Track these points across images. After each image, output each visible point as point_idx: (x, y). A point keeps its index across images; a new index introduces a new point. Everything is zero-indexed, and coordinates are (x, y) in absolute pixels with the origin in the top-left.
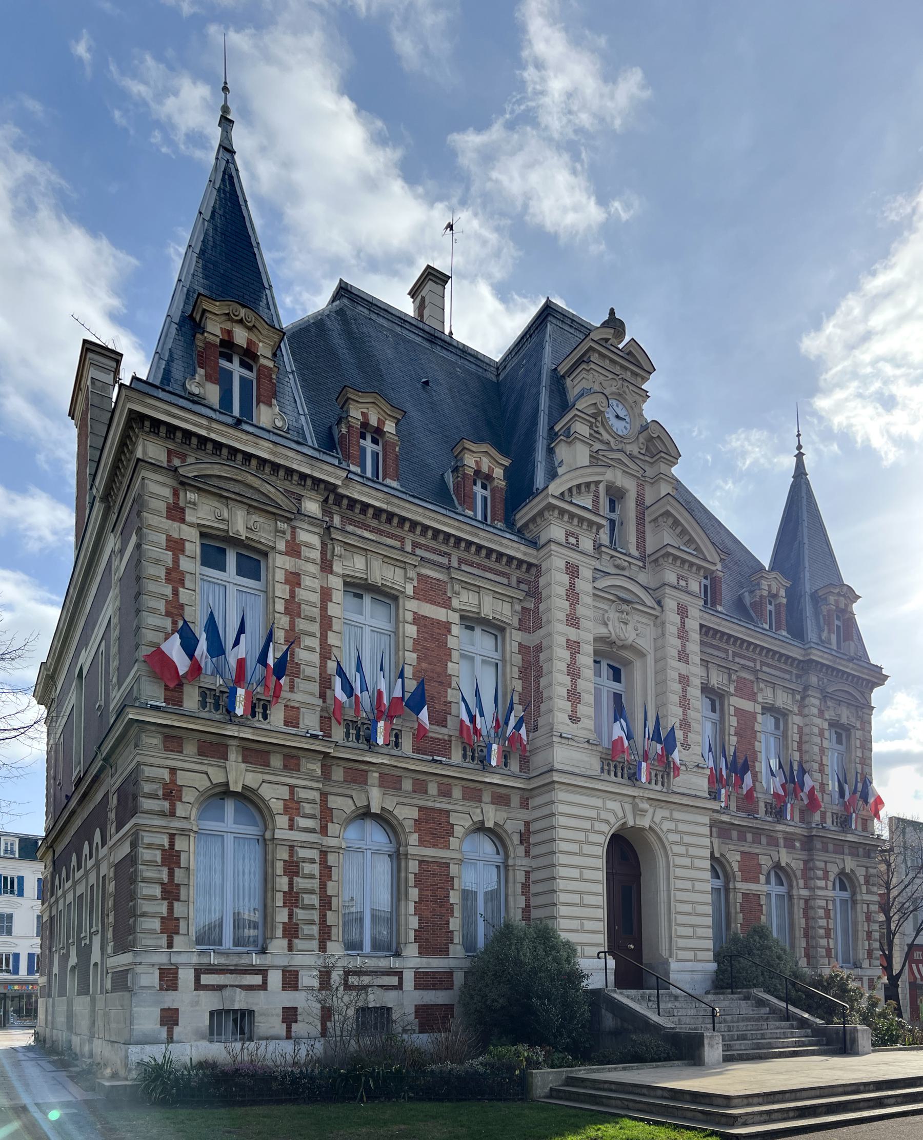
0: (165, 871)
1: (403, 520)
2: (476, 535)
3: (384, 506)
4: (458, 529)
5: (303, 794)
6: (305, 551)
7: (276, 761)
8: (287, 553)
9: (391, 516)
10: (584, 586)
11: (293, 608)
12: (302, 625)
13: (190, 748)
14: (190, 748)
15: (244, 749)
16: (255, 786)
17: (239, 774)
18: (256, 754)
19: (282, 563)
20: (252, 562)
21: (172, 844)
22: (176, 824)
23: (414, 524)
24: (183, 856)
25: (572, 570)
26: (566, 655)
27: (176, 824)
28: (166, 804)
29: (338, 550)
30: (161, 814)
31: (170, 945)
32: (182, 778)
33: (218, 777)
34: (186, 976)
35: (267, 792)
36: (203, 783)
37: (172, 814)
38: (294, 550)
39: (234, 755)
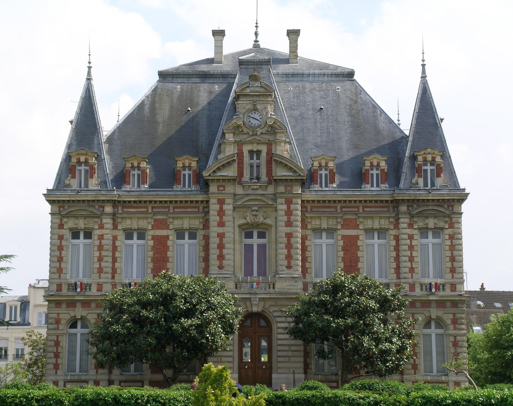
0: (55, 348)
1: (145, 202)
2: (177, 198)
3: (136, 199)
4: (169, 198)
6: (106, 226)
7: (93, 305)
8: (99, 228)
9: (140, 202)
10: (228, 207)
11: (100, 248)
12: (104, 253)
13: (64, 306)
14: (64, 306)
15: (82, 303)
16: (85, 315)
18: (86, 304)
19: (97, 233)
20: (88, 235)
21: (57, 339)
22: (58, 332)
23: (150, 202)
24: (61, 343)
25: (221, 202)
26: (217, 240)
27: (58, 332)
28: (56, 326)
29: (119, 220)
30: (54, 329)
31: (56, 373)
32: (61, 316)
33: (72, 314)
35: (89, 317)
36: (68, 317)
37: (58, 329)
38: (101, 227)
39: (79, 305)
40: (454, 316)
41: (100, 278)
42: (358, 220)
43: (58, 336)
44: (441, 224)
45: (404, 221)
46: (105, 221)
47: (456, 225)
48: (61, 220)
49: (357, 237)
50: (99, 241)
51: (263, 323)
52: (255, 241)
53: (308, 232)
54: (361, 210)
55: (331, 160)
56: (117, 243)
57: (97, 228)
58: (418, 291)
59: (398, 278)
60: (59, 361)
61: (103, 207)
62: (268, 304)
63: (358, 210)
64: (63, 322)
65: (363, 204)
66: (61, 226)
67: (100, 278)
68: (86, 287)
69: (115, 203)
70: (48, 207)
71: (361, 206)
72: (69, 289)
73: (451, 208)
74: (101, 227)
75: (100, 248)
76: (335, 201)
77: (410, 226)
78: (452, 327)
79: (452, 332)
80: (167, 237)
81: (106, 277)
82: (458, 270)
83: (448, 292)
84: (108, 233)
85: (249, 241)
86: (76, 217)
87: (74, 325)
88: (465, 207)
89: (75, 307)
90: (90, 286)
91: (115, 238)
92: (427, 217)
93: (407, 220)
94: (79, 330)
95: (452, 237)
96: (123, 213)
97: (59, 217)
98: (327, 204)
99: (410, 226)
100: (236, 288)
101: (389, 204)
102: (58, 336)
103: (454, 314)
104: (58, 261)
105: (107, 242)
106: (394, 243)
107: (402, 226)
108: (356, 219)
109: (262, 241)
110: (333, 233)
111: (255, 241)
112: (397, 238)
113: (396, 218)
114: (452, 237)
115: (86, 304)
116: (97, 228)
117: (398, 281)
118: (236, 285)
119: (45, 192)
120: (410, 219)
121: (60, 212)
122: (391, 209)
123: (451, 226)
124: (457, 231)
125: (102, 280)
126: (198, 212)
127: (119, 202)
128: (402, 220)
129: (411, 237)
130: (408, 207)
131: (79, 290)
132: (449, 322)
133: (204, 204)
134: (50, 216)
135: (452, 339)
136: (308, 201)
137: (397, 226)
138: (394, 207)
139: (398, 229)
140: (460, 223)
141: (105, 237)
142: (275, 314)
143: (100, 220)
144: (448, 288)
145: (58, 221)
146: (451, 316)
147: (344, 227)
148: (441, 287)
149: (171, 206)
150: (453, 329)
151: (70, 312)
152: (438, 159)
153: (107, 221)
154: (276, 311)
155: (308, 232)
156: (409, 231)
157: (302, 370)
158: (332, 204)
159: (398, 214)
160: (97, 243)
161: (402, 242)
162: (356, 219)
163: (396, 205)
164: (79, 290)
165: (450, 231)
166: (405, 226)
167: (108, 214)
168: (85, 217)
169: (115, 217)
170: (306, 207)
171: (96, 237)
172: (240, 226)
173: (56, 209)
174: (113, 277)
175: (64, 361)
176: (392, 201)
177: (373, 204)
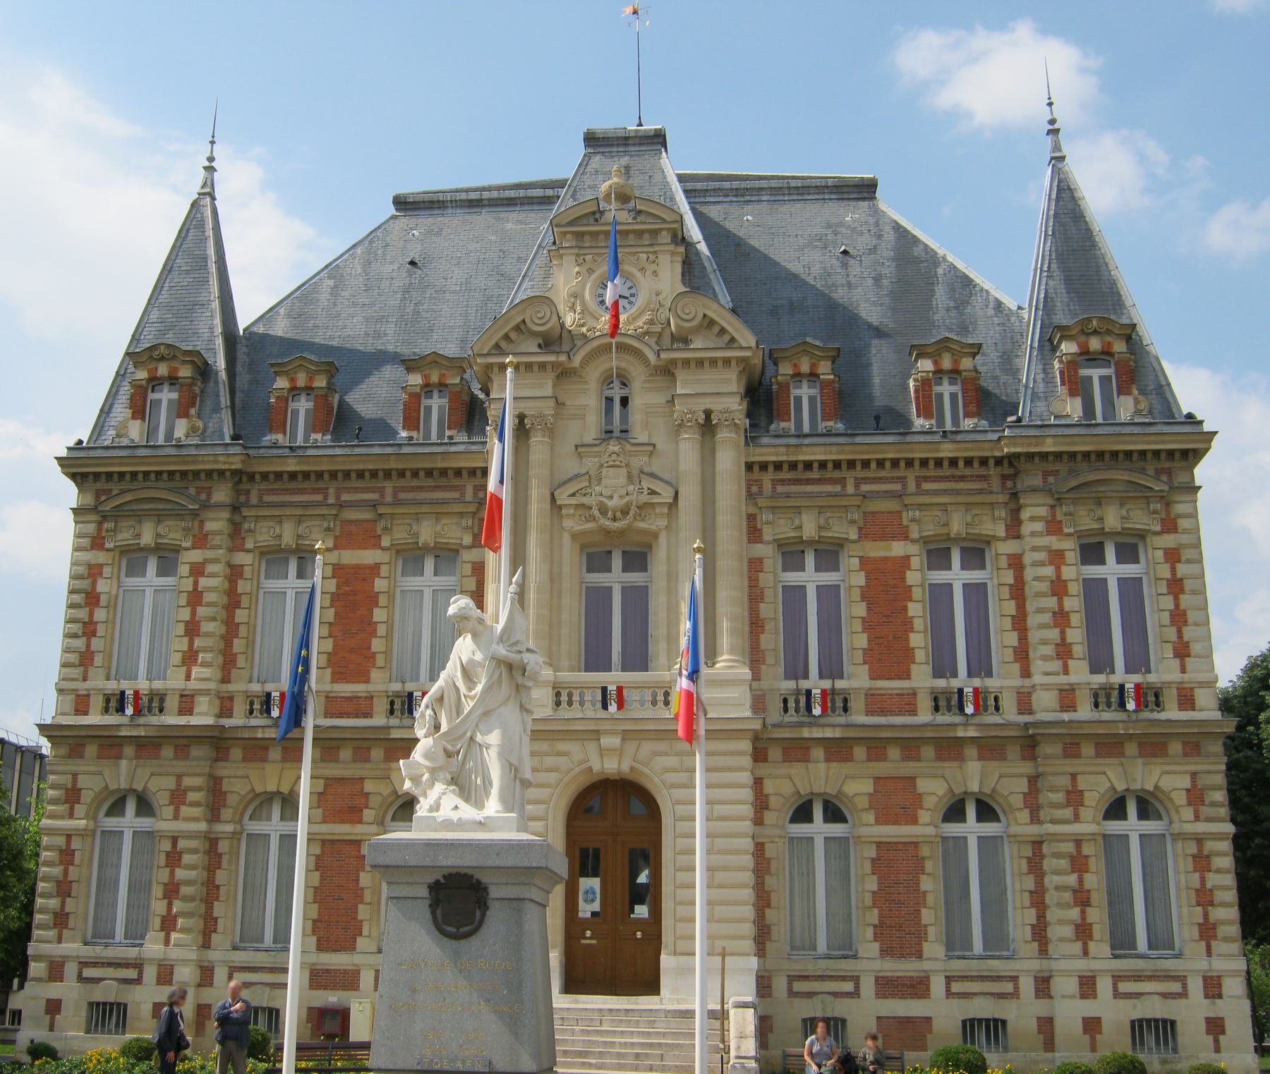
5: (187, 781)
17: (124, 773)
34: (71, 969)
40: (1193, 781)
41: (188, 677)
42: (904, 514)
43: (69, 837)
44: (1140, 519)
45: (1034, 511)
46: (210, 526)
47: (1183, 524)
48: (100, 524)
49: (905, 561)
50: (191, 580)
51: (637, 807)
52: (616, 578)
53: (764, 550)
54: (912, 486)
55: (823, 358)
56: (242, 586)
57: (189, 544)
58: (1084, 712)
59: (1026, 673)
60: (70, 905)
61: (209, 492)
62: (647, 747)
63: (905, 486)
64: (87, 796)
65: (917, 471)
66: (97, 543)
67: (188, 677)
68: (151, 701)
69: (240, 478)
70: (70, 493)
71: (911, 476)
72: (106, 710)
73: (1164, 478)
74: (201, 541)
75: (195, 598)
76: (837, 465)
77: (1054, 527)
78: (1188, 813)
79: (1190, 828)
80: (375, 569)
81: (204, 674)
82: (1195, 648)
83: (1172, 713)
84: (216, 559)
85: (598, 578)
86: (139, 517)
87: (117, 808)
88: (1203, 472)
89: (119, 757)
90: (162, 700)
91: (235, 573)
92: (1099, 502)
93: (1043, 511)
94: (129, 821)
95: (1173, 556)
96: (262, 505)
97: (95, 518)
98: (815, 474)
99: (1054, 527)
100: (558, 704)
101: (992, 471)
102: (69, 837)
103: (1194, 775)
104: (84, 634)
105: (212, 583)
106: (1009, 577)
107: (1027, 528)
108: (900, 512)
109: (636, 578)
110: (836, 554)
111: (616, 578)
112: (1016, 563)
113: (1012, 506)
114: (1173, 556)
115: (148, 746)
116: (189, 544)
117: (1027, 682)
118: (558, 694)
119: (64, 453)
120: (1053, 507)
121: (98, 502)
122: (996, 484)
123: (1170, 526)
124: (1183, 539)
125: (193, 685)
126: (461, 500)
127: (251, 477)
128: (1025, 514)
129: (1057, 558)
130: (1046, 474)
131: (129, 711)
132: (1180, 798)
133: (478, 481)
134: (71, 516)
135: (1192, 848)
136: (764, 466)
137: (1014, 531)
138: (1004, 477)
139: (1018, 537)
140: (1194, 515)
141: (210, 568)
142: (671, 778)
143: (196, 523)
144: (1170, 698)
145: (91, 528)
146: (1186, 782)
147: (864, 535)
148: (1152, 699)
149: (389, 486)
150: (1192, 818)
151: (106, 774)
152: (1119, 347)
153: (217, 524)
154: (674, 770)
155: (764, 550)
156: (1054, 542)
157: (749, 945)
158: (830, 473)
159: (1015, 495)
160: (188, 584)
161: (1029, 574)
162: (900, 512)
163: (1012, 471)
164: (129, 711)
165: (1169, 540)
166: (1039, 526)
167: (219, 506)
168: (160, 517)
169: (237, 518)
170: (759, 483)
171: (184, 570)
172: (575, 536)
173: (89, 500)
174: (225, 680)
175: (82, 906)
176: (999, 461)
177: (946, 471)
